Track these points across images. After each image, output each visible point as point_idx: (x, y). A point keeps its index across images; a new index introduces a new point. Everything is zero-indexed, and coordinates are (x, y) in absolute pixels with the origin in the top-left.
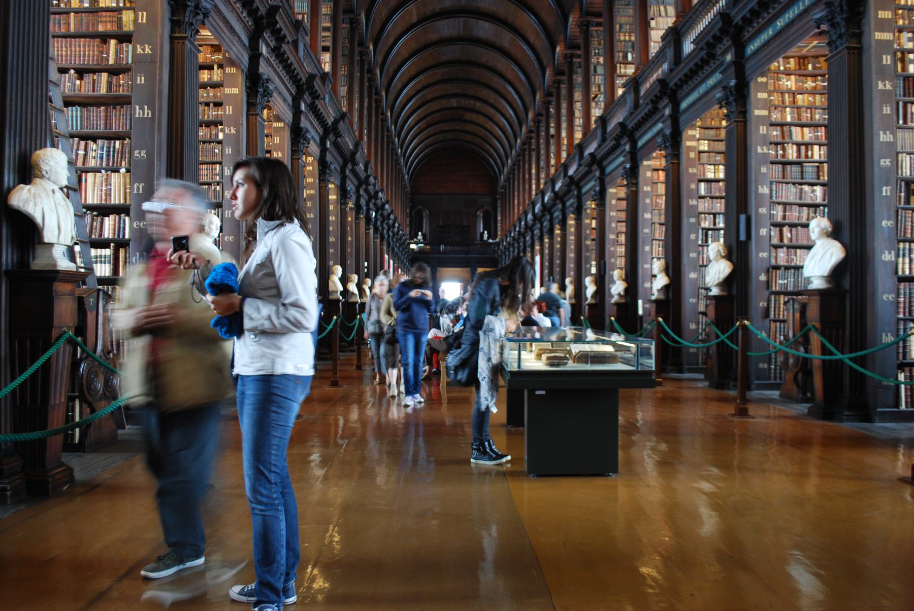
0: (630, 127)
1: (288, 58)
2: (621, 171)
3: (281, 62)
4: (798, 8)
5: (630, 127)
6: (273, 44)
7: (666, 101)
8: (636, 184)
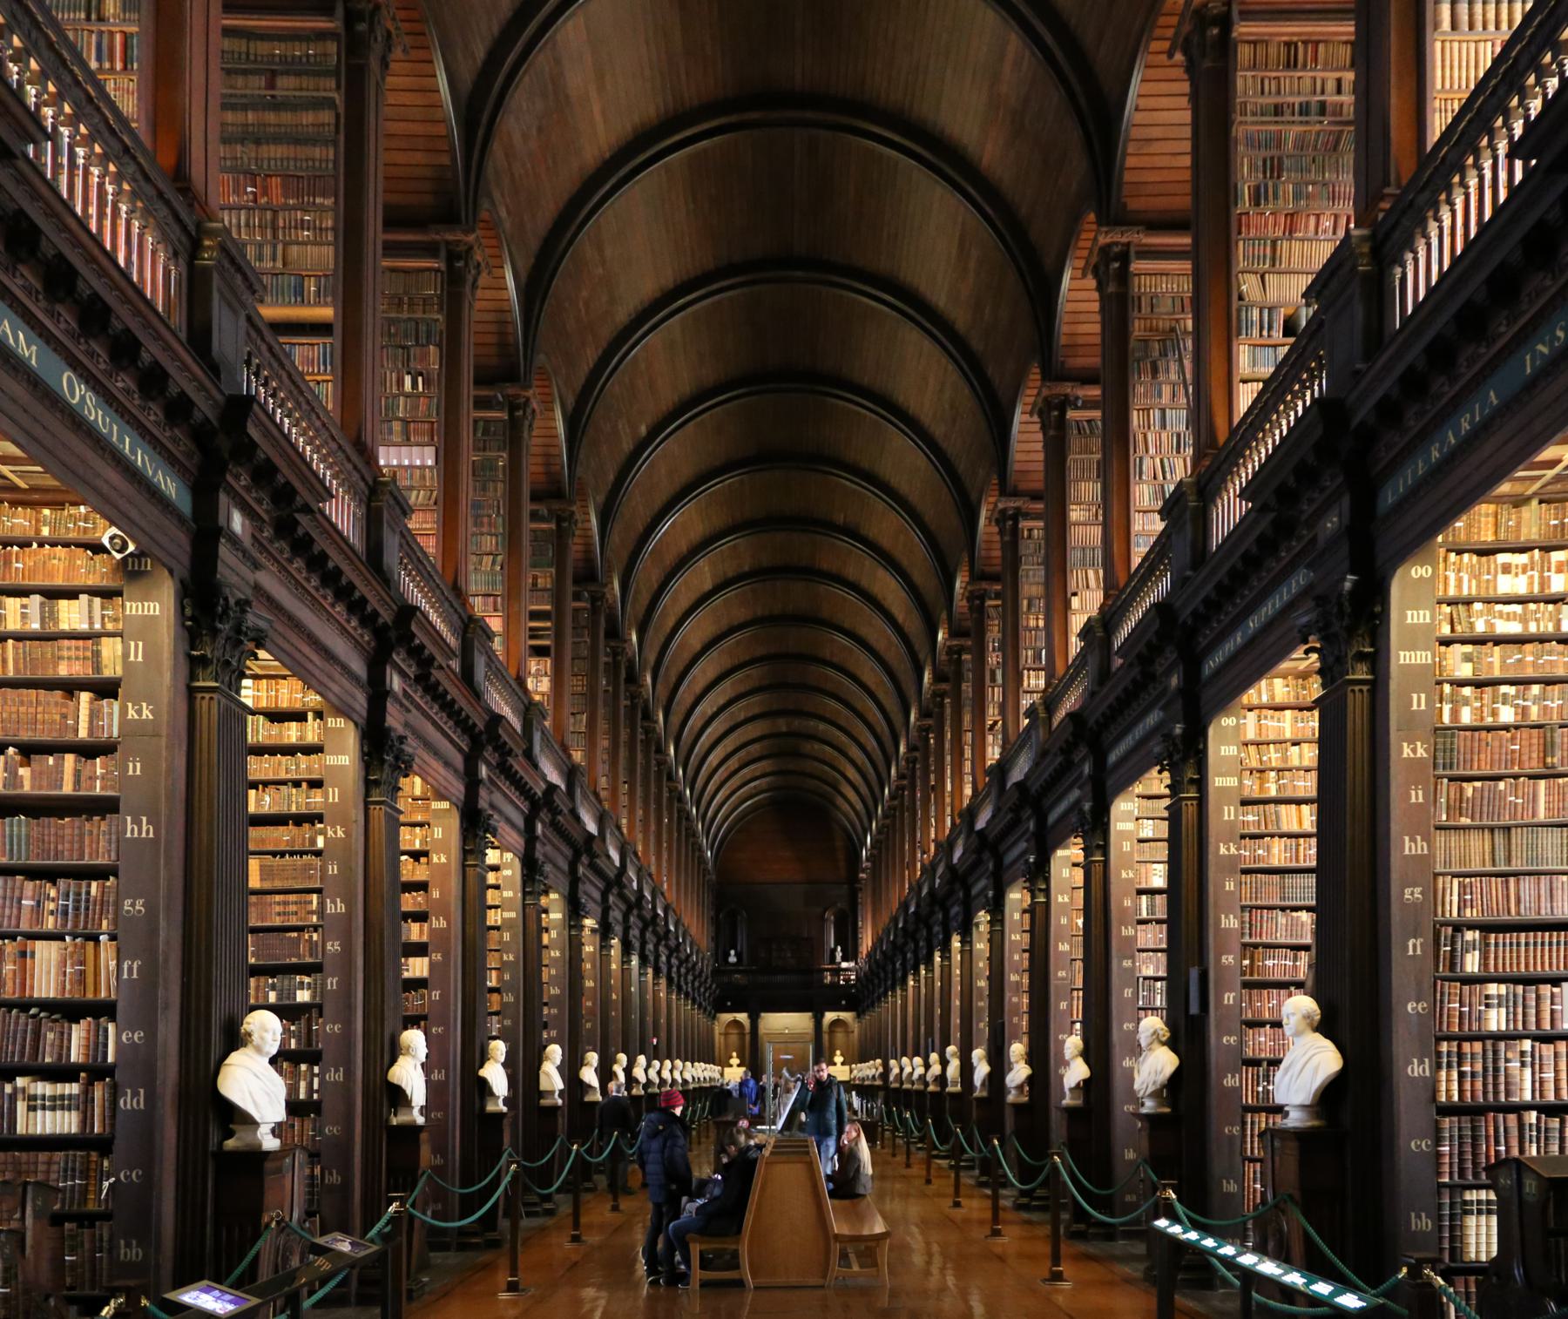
0: (1033, 790)
1: (446, 692)
2: (1020, 866)
3: (434, 699)
4: (1281, 598)
5: (1033, 790)
8: (1047, 892)
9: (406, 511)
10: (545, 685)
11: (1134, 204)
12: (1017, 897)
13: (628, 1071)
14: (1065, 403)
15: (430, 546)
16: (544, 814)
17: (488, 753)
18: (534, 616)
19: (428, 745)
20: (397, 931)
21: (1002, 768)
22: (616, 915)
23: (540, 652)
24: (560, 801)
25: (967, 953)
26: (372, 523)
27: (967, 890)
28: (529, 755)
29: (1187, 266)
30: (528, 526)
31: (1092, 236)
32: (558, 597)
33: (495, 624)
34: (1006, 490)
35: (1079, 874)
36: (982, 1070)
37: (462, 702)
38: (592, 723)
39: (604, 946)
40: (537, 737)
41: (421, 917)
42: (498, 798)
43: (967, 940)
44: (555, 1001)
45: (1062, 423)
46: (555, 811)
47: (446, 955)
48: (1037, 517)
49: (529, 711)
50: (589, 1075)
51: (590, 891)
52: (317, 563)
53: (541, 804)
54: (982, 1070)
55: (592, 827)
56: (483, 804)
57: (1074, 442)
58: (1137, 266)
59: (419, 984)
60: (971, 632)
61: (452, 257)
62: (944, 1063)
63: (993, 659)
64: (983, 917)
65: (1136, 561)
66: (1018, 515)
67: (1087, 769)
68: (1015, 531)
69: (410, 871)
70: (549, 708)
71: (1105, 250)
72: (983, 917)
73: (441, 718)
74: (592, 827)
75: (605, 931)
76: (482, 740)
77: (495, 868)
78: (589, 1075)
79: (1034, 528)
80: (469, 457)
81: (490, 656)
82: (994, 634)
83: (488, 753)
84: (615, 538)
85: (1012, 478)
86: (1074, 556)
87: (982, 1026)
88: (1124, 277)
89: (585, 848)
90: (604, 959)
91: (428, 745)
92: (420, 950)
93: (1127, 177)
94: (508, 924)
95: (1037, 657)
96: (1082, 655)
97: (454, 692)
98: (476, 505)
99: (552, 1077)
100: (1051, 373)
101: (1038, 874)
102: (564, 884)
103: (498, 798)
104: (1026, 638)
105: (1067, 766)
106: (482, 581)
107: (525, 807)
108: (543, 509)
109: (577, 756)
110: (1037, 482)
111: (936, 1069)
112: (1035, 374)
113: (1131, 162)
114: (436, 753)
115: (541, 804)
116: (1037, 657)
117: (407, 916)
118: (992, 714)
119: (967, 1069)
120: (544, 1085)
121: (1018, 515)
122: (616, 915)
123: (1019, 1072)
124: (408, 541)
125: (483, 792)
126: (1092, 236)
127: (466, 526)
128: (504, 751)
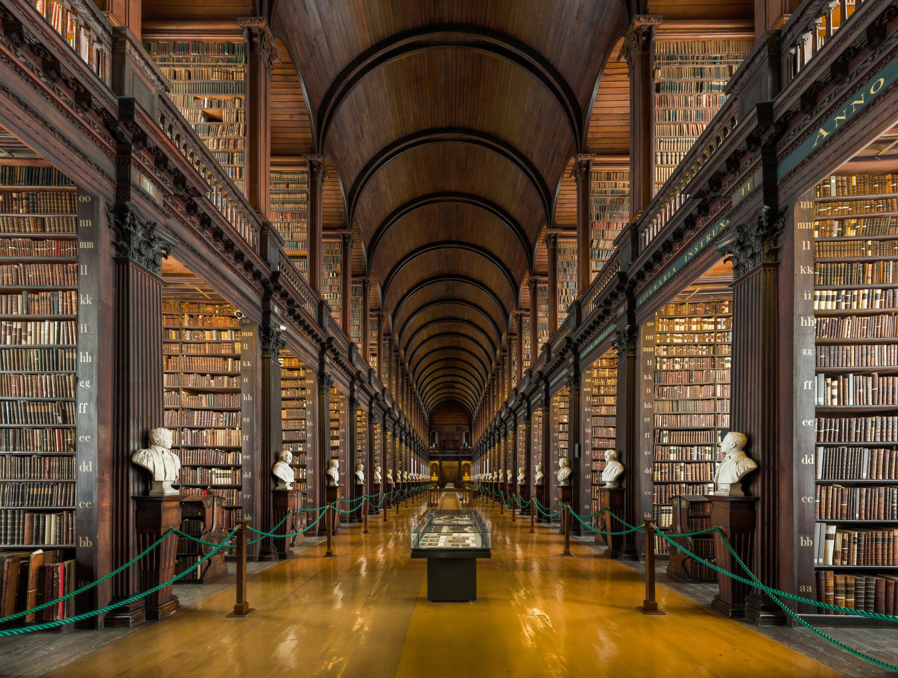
6: (333, 356)
7: (542, 382)
8: (530, 424)
9: (330, 311)
10: (376, 364)
11: (559, 222)
12: (522, 426)
13: (402, 476)
14: (536, 282)
15: (339, 322)
16: (375, 401)
17: (357, 382)
18: (371, 344)
19: (338, 379)
20: (329, 433)
21: (516, 390)
22: (398, 431)
23: (374, 355)
24: (380, 396)
25: (506, 443)
27: (506, 425)
28: (370, 383)
29: (575, 240)
30: (369, 318)
31: (545, 231)
32: (379, 339)
33: (360, 346)
34: (518, 308)
35: (541, 420)
36: (510, 476)
37: (348, 366)
38: (390, 376)
39: (394, 440)
40: (372, 379)
41: (337, 429)
42: (360, 395)
43: (506, 439)
44: (379, 455)
45: (535, 288)
46: (378, 400)
47: (345, 440)
48: (528, 316)
49: (370, 371)
50: (390, 476)
51: (389, 424)
53: (373, 398)
54: (510, 476)
55: (390, 406)
56: (355, 397)
57: (539, 293)
58: (559, 240)
59: (335, 448)
60: (507, 351)
61: (345, 238)
62: (498, 474)
63: (514, 358)
64: (510, 432)
65: (559, 327)
66: (521, 315)
67: (543, 388)
68: (521, 320)
69: (333, 415)
70: (376, 369)
71: (549, 236)
72: (510, 432)
73: (342, 371)
74: (390, 406)
75: (394, 435)
76: (355, 378)
77: (359, 416)
78: (390, 476)
79: (527, 320)
80: (350, 297)
81: (358, 355)
82: (514, 350)
83: (357, 382)
84: (397, 322)
85: (520, 305)
86: (539, 327)
87: (510, 464)
88: (555, 243)
89: (387, 412)
90: (394, 444)
91: (338, 379)
92: (337, 438)
93: (556, 214)
94: (364, 432)
95: (528, 357)
96: (542, 355)
97: (346, 363)
98: (352, 312)
99: (378, 476)
100: (533, 273)
101: (528, 419)
102: (381, 422)
103: (360, 395)
104: (524, 352)
105: (537, 387)
106: (354, 332)
107: (369, 398)
108: (373, 313)
109: (386, 386)
110: (528, 306)
111: (496, 476)
112: (527, 274)
113: (557, 210)
114: (341, 381)
115: (373, 398)
116: (528, 357)
117: (332, 429)
118: (514, 374)
119: (505, 476)
120: (375, 478)
121: (521, 315)
122: (398, 431)
123: (520, 477)
124: (331, 320)
125: (355, 393)
126: (545, 231)
127: (350, 317)
128: (362, 381)
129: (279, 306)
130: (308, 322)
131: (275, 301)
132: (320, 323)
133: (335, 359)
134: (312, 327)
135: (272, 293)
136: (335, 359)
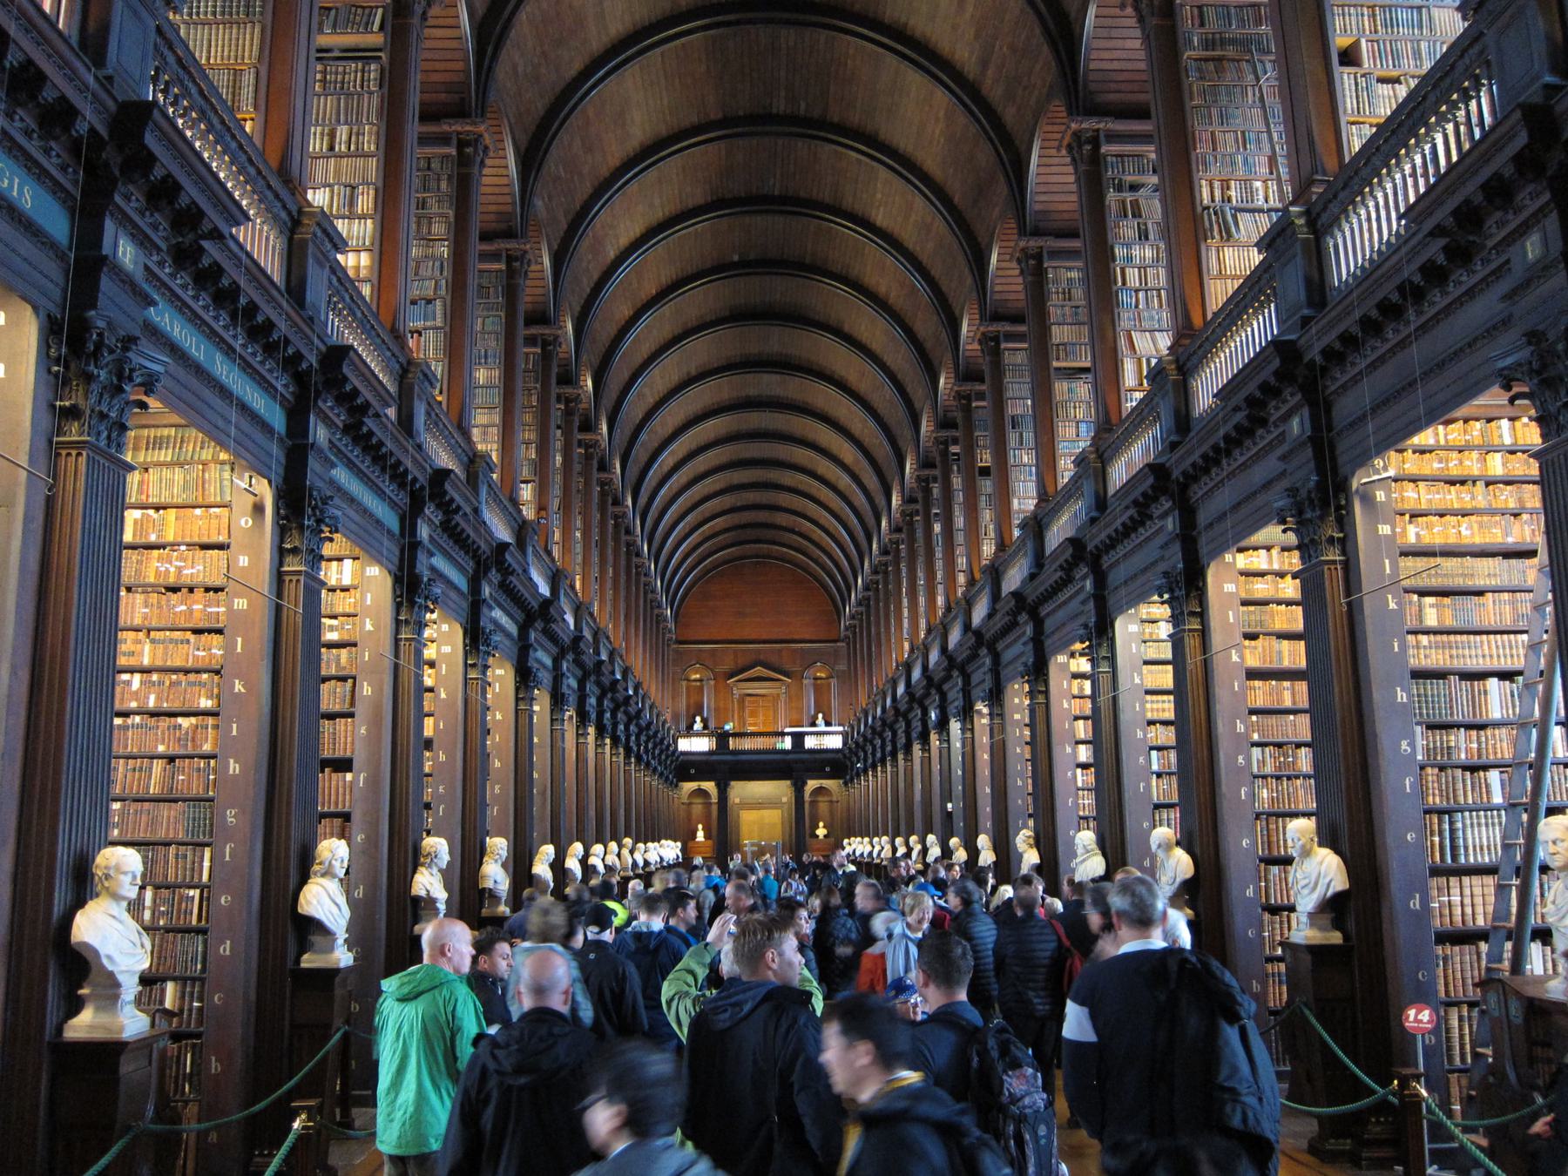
6: (341, 418)
26: (294, 255)
52: (225, 297)
81: (431, 405)
129: (142, 241)
130: (249, 292)
131: (125, 221)
132: (296, 289)
133: (347, 429)
134: (267, 311)
135: (114, 182)
136: (347, 429)
